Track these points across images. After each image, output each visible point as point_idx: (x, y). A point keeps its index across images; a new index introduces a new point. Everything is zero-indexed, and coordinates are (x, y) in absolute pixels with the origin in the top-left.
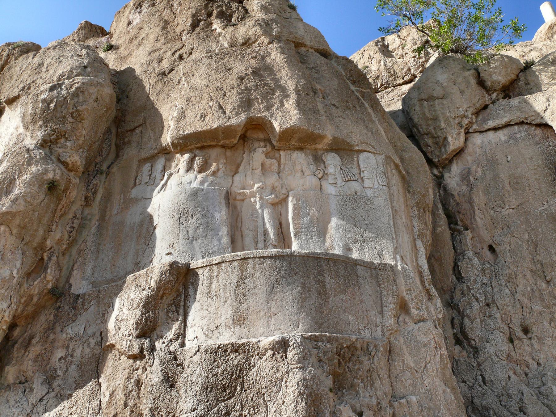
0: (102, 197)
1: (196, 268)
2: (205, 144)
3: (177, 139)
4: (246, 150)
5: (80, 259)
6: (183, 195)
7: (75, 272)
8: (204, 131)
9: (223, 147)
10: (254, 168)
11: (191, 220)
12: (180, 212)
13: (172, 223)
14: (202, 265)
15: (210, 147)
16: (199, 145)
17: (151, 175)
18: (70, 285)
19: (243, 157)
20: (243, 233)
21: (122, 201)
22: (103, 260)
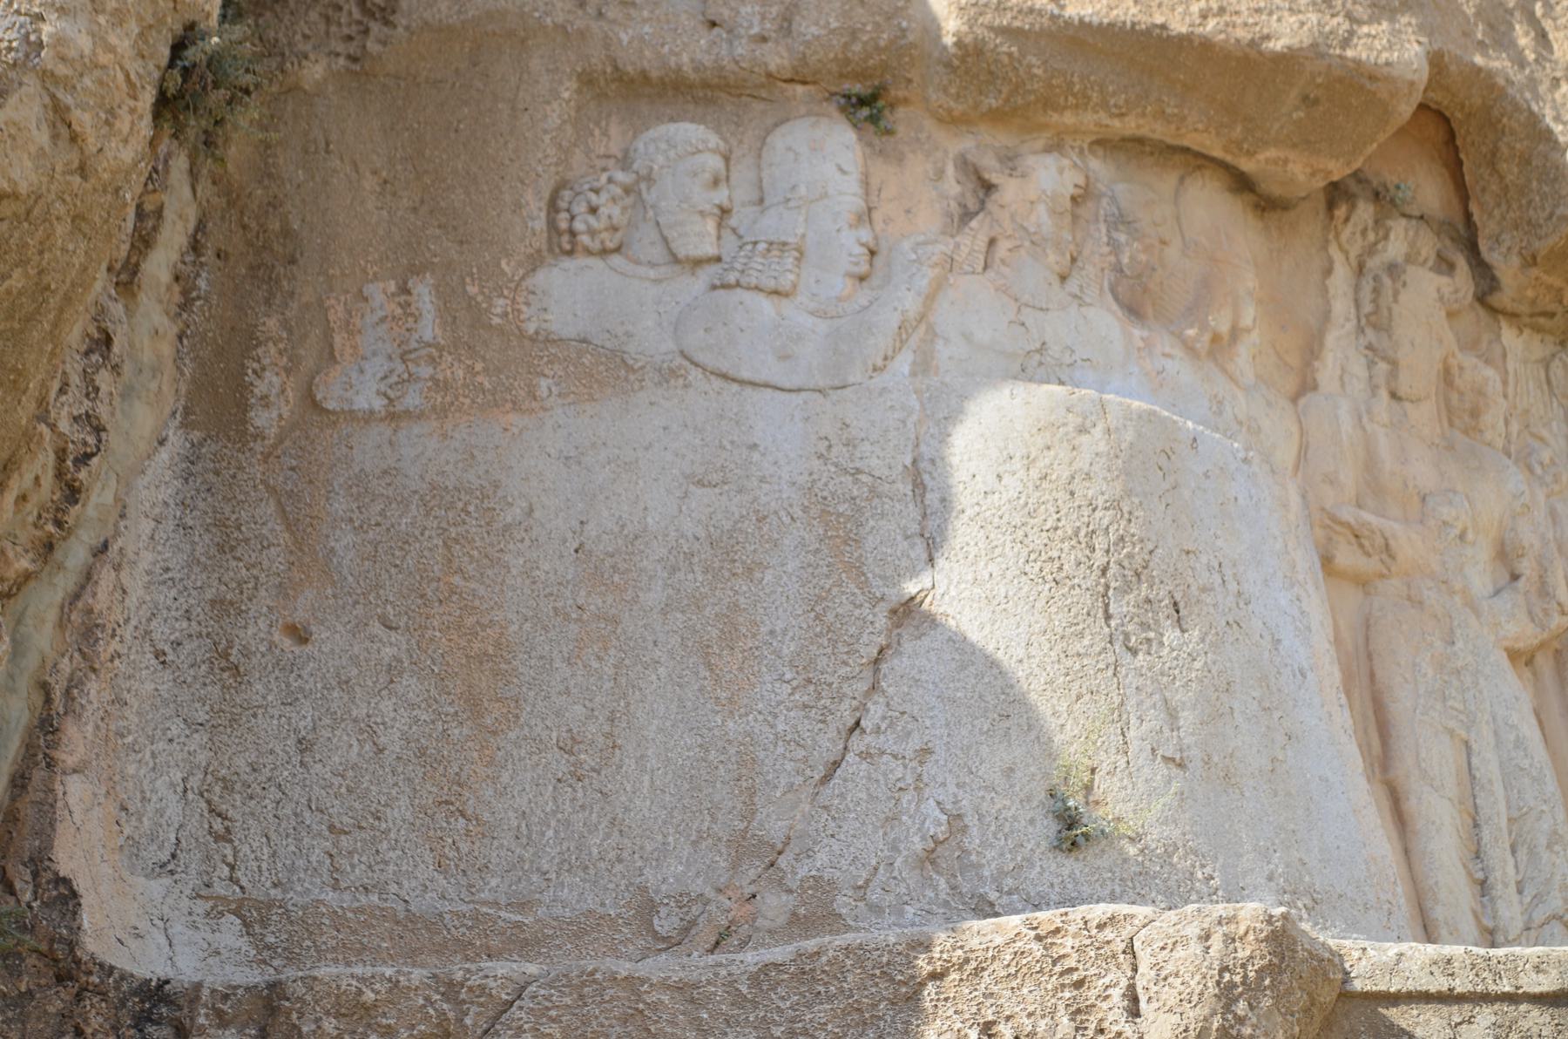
0: (195, 246)
1: (1394, 999)
2: (1159, 131)
3: (1005, 31)
4: (1334, 250)
5: (93, 686)
6: (1095, 441)
7: (75, 791)
8: (1206, 45)
9: (1242, 183)
10: (1403, 390)
11: (1171, 635)
12: (1099, 559)
13: (1060, 621)
14: (1439, 984)
15: (1197, 161)
16: (1130, 126)
17: (724, 212)
18: (67, 897)
19: (1325, 290)
20: (1410, 805)
21: (429, 328)
22: (305, 746)
